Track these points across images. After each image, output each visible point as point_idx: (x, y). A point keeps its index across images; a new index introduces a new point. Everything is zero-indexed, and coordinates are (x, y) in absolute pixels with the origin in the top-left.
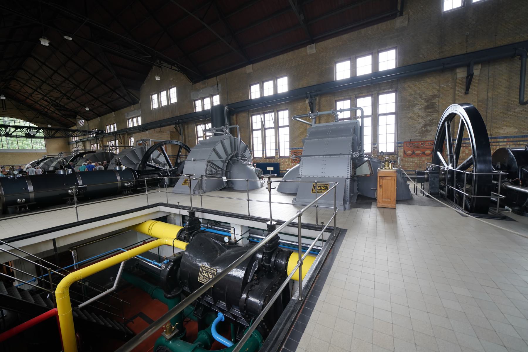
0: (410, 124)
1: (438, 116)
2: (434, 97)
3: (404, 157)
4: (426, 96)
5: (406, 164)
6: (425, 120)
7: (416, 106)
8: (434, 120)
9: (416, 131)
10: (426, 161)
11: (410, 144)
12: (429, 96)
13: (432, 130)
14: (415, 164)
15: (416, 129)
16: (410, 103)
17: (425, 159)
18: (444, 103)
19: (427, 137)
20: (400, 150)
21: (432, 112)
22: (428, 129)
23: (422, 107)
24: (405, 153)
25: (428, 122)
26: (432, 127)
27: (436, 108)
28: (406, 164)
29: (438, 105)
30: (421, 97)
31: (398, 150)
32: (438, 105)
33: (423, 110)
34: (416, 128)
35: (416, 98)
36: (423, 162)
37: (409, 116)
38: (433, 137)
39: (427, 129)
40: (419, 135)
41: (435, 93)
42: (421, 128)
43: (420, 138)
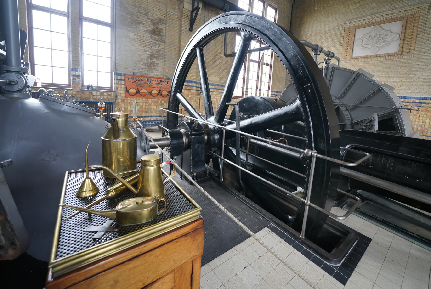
0: (133, 48)
1: (165, 48)
2: (161, 21)
3: (125, 97)
4: (153, 17)
5: (129, 107)
6: (151, 49)
7: (141, 25)
8: (161, 52)
9: (141, 61)
10: (152, 104)
11: (133, 79)
12: (155, 18)
13: (158, 64)
14: (140, 107)
15: (141, 58)
16: (133, 17)
17: (152, 101)
18: (170, 33)
19: (153, 73)
20: (120, 85)
21: (159, 41)
22: (154, 62)
23: (148, 30)
24: (127, 91)
25: (154, 52)
26: (159, 60)
27: (163, 37)
28: (129, 107)
29: (164, 33)
30: (147, 14)
31: (117, 85)
32: (164, 33)
33: (149, 35)
34: (141, 57)
35: (141, 13)
36: (150, 105)
37: (132, 37)
38: (160, 74)
39: (153, 61)
40: (145, 68)
41: (163, 18)
42: (146, 58)
43: (146, 72)
